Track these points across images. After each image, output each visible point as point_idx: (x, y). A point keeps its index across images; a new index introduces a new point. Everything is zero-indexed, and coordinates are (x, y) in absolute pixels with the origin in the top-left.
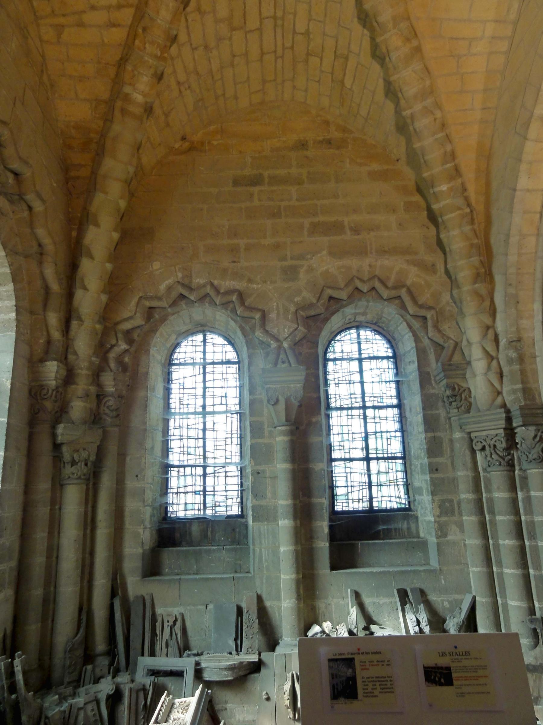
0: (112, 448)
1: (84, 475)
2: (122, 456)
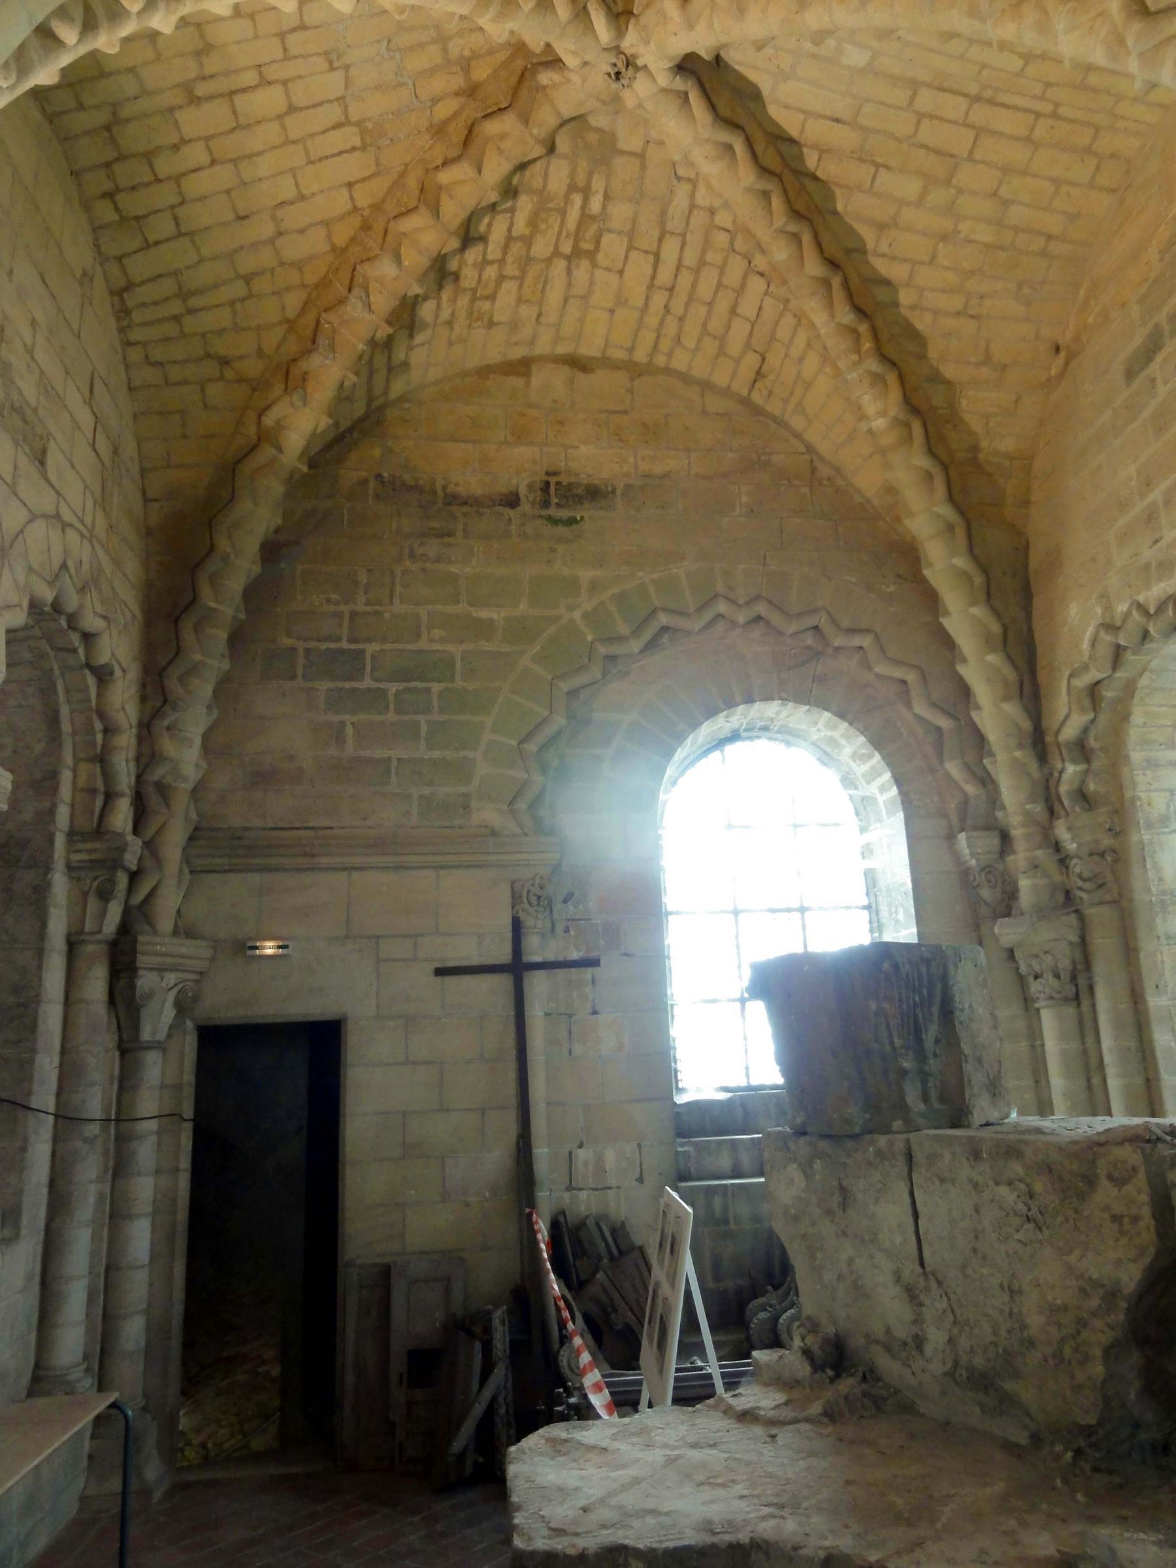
0: (1104, 945)
1: (1059, 992)
2: (1129, 951)
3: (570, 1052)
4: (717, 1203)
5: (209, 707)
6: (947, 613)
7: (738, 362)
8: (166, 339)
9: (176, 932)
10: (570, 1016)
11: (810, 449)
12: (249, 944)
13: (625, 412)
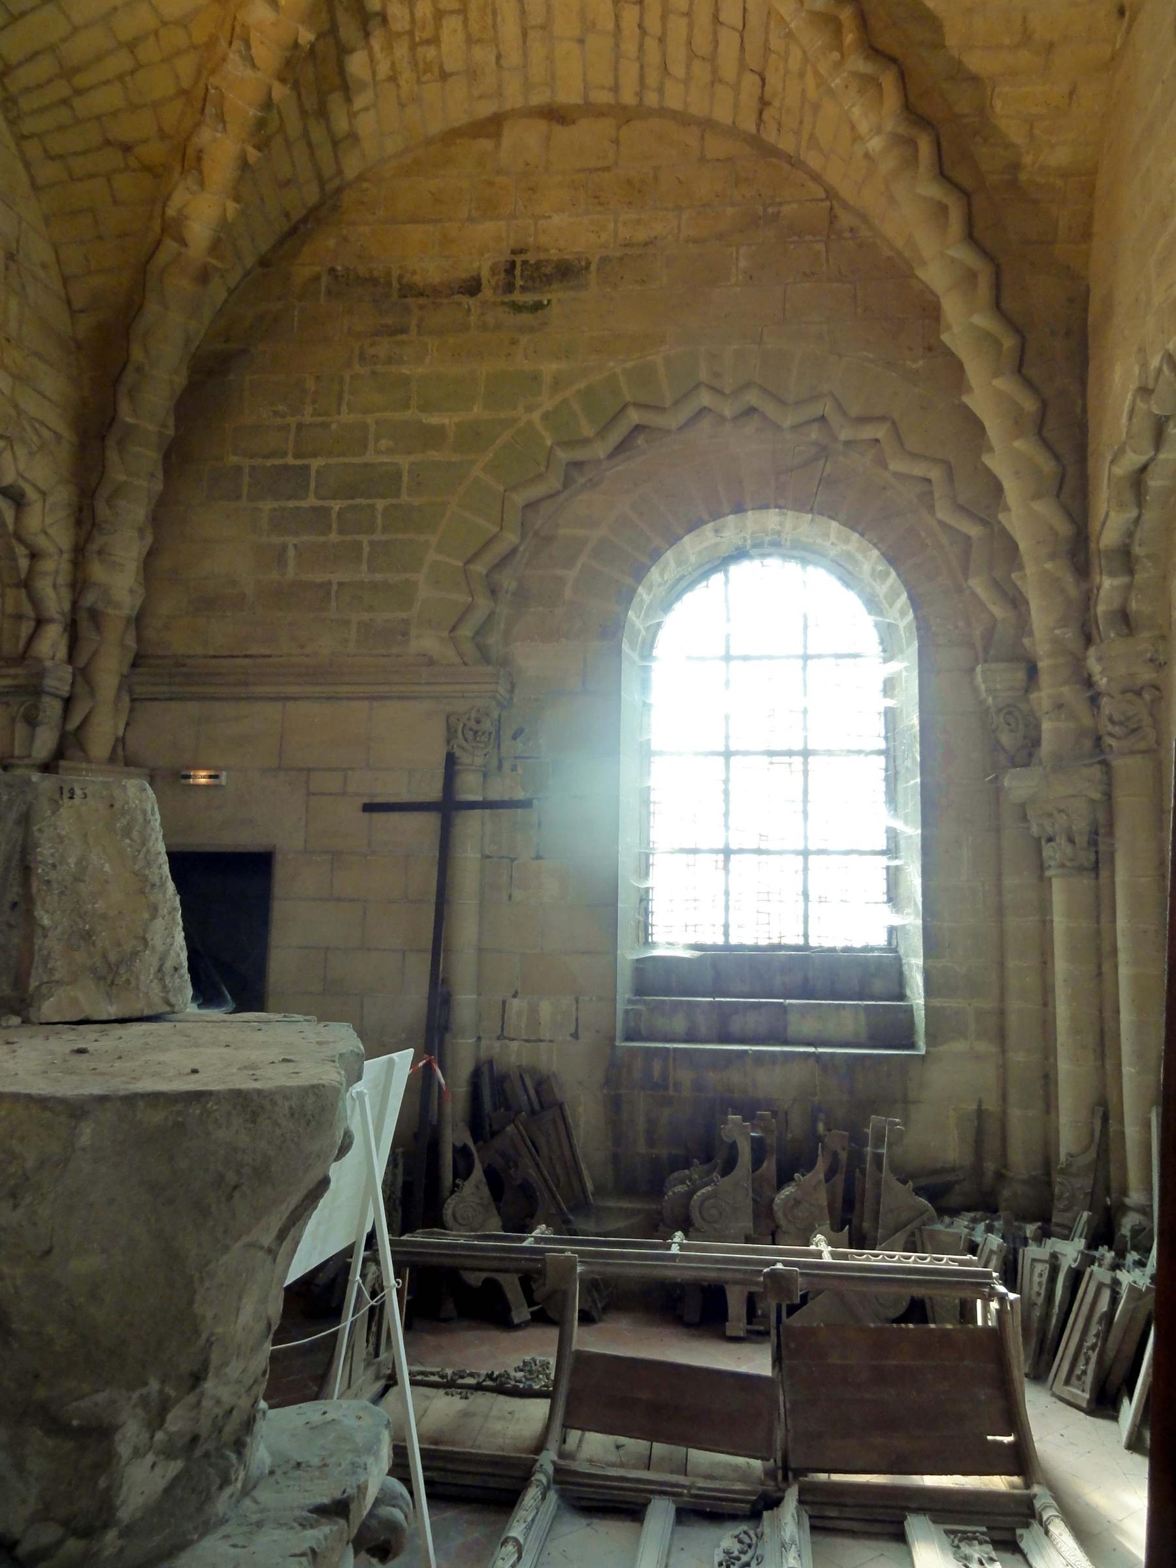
3: (510, 897)
4: (657, 1067)
5: (141, 531)
6: (969, 390)
7: (736, 87)
8: (61, 128)
9: (112, 759)
10: (513, 860)
11: (831, 194)
12: (184, 773)
13: (607, 169)
